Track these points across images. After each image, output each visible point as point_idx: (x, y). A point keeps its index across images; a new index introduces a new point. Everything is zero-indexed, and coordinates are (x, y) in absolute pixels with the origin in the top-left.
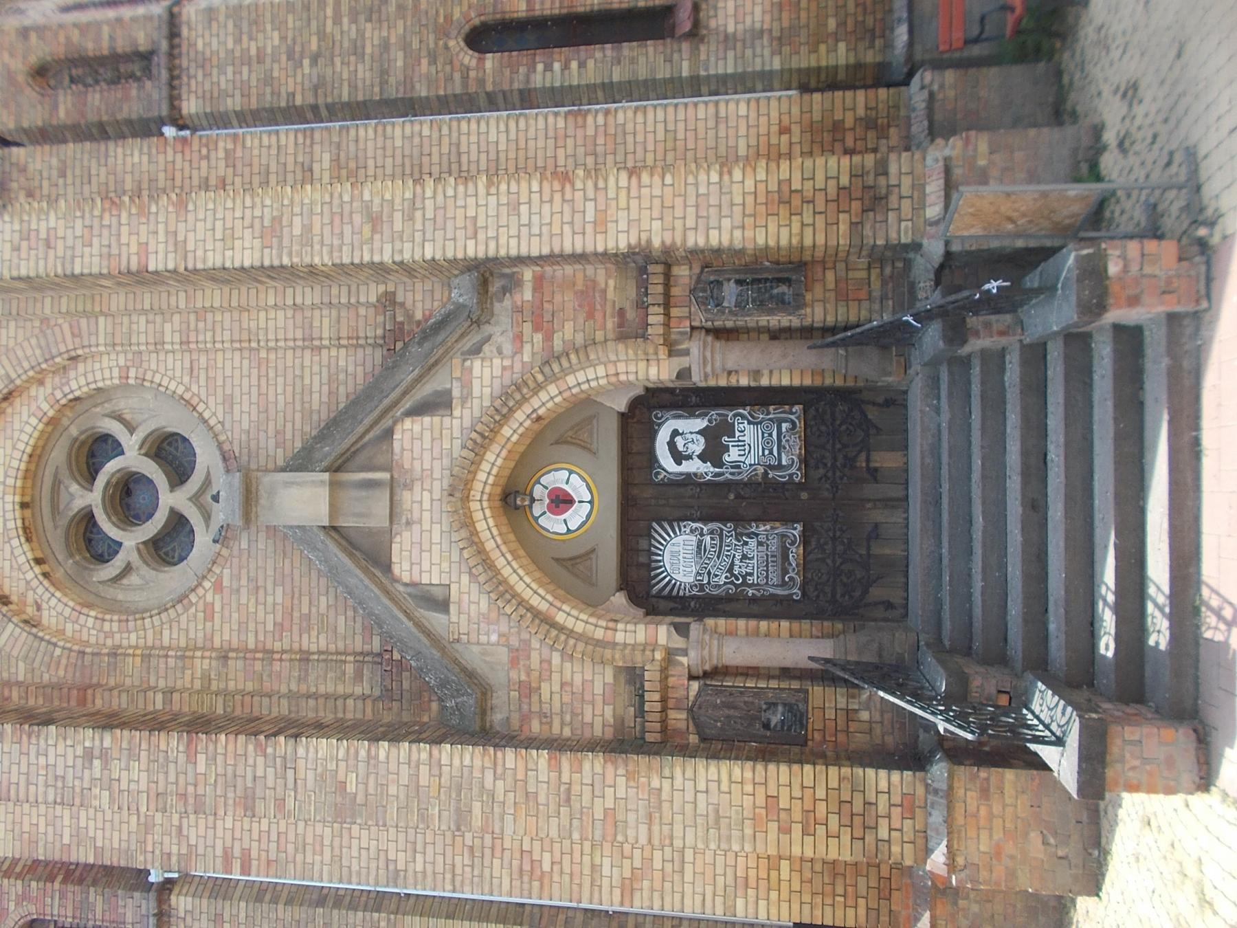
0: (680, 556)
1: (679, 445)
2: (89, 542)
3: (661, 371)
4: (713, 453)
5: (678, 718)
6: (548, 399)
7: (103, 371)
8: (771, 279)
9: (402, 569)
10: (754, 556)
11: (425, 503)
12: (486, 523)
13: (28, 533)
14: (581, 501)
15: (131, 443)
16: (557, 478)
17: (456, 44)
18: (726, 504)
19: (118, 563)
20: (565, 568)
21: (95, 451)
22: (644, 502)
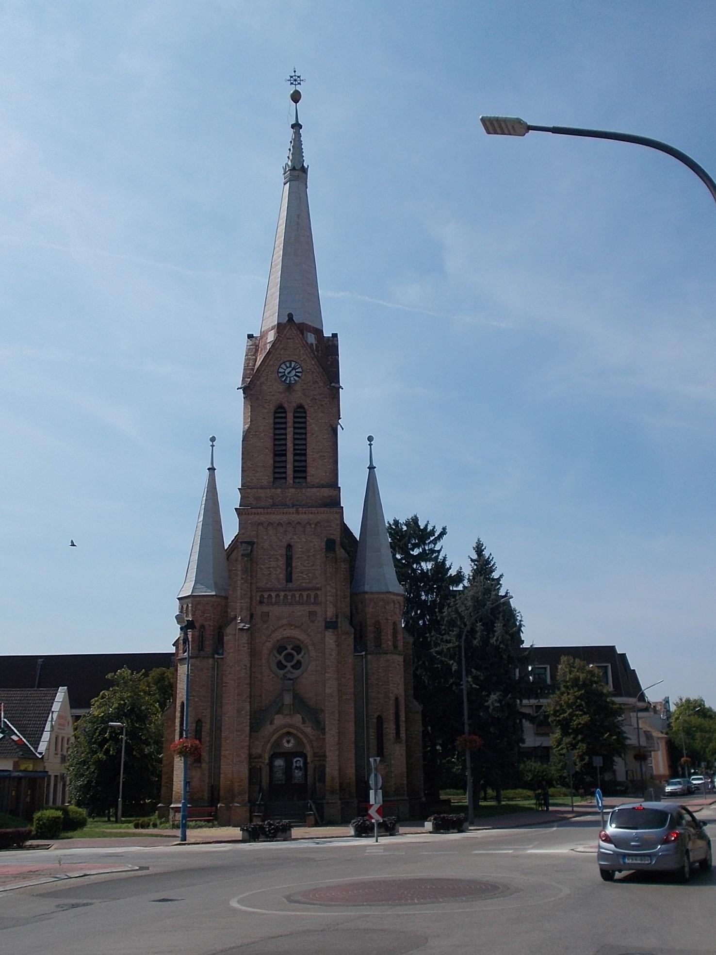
0: (279, 762)
1: (298, 762)
2: (281, 649)
3: (309, 760)
4: (297, 768)
5: (254, 764)
6: (305, 741)
7: (313, 653)
8: (322, 778)
9: (276, 716)
10: (279, 775)
11: (288, 720)
12: (285, 730)
13: (283, 638)
14: (288, 745)
15: (299, 657)
16: (292, 741)
17: (378, 713)
18: (288, 770)
19: (277, 655)
20: (278, 743)
21: (298, 649)
22: (289, 756)
